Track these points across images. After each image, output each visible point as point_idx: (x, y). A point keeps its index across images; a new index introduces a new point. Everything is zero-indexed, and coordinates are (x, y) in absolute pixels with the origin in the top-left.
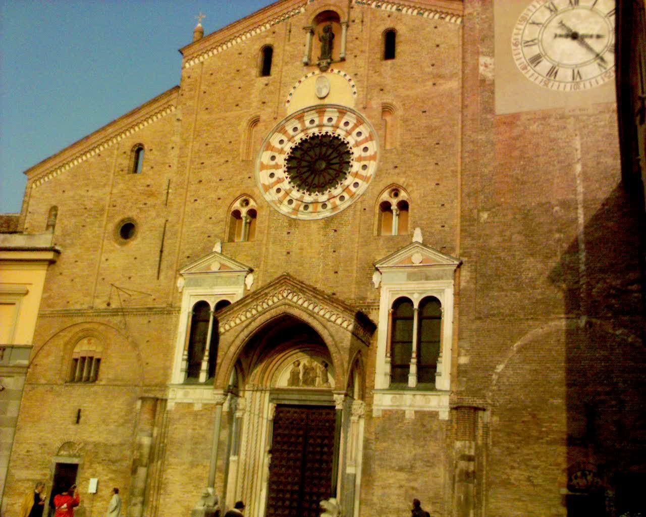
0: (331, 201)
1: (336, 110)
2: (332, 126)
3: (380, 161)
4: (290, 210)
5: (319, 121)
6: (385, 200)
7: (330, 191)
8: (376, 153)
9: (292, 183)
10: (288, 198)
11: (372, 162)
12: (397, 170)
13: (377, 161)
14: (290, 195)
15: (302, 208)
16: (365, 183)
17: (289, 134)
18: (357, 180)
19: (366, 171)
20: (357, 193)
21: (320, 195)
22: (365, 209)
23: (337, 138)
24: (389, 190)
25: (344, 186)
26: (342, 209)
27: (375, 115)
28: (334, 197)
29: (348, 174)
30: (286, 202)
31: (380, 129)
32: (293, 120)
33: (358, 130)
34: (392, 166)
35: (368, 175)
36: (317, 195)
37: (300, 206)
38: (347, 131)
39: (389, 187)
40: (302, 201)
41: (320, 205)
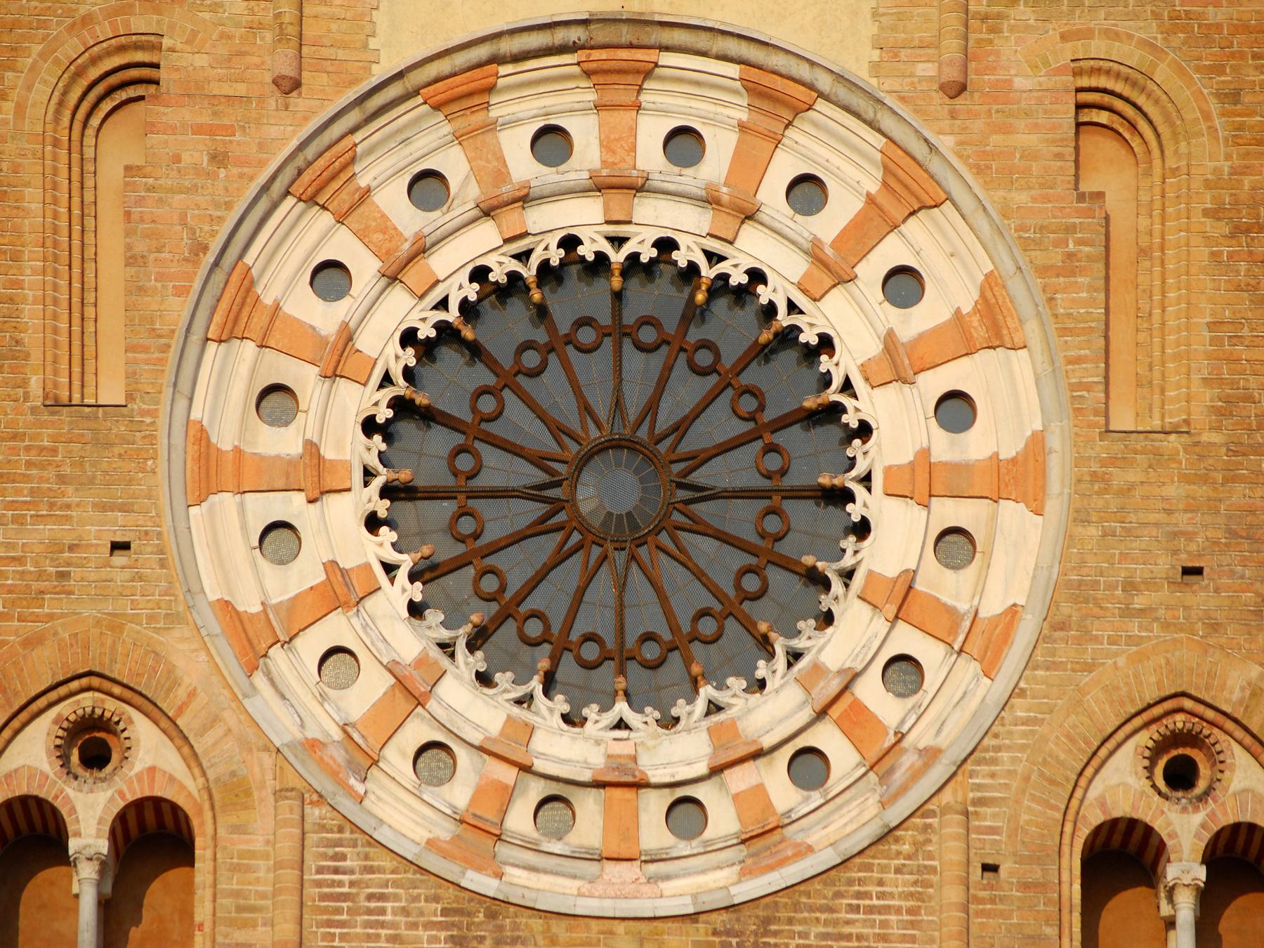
0: (740, 779)
1: (733, 70)
2: (710, 200)
3: (1080, 517)
4: (445, 831)
5: (606, 145)
6: (1122, 809)
7: (714, 708)
8: (1037, 443)
9: (434, 617)
10: (417, 732)
11: (1012, 513)
12: (1200, 597)
13: (1055, 505)
14: (432, 705)
15: (520, 819)
16: (968, 669)
17: (385, 226)
18: (907, 640)
19: (971, 571)
20: (920, 736)
21: (643, 722)
22: (990, 868)
23: (743, 294)
24: (1145, 739)
25: (818, 669)
26: (827, 858)
27: (1029, 155)
28: (758, 754)
29: (837, 586)
30: (398, 758)
31: (1070, 268)
32: (415, 109)
33: (891, 253)
34: (1165, 565)
35: (992, 607)
36: (621, 725)
37: (507, 796)
38: (815, 253)
39: (1144, 715)
40: (526, 769)
41: (654, 805)
